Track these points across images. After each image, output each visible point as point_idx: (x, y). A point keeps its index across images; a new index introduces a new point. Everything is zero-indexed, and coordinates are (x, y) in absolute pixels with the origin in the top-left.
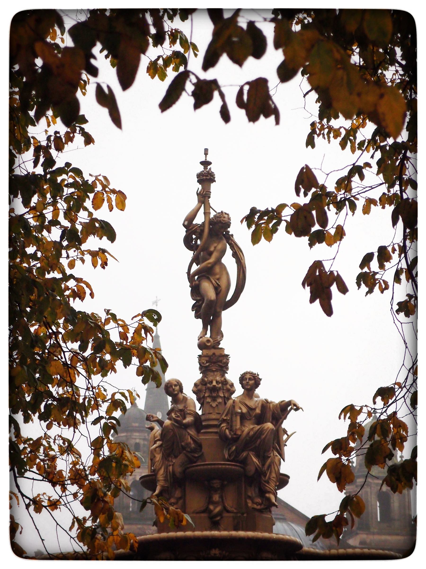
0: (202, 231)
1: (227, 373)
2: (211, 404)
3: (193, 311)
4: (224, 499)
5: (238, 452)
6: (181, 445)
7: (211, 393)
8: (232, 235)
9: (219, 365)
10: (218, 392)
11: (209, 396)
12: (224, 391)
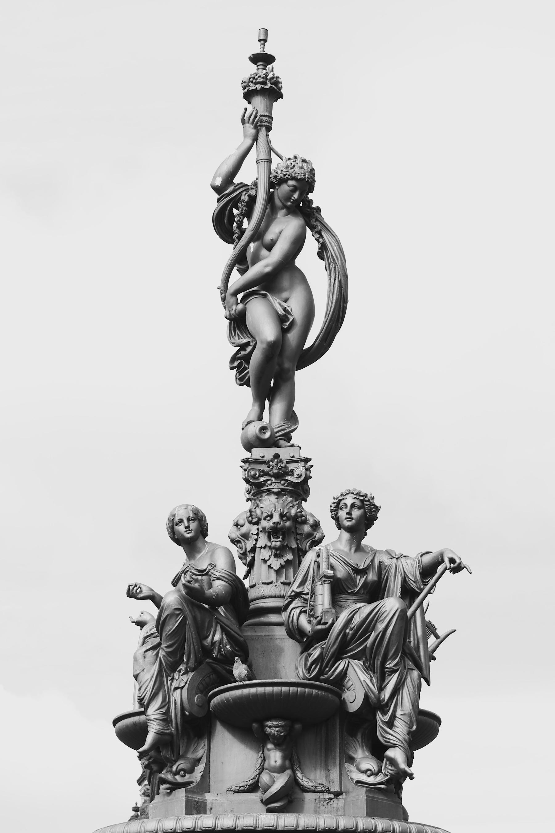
0: (253, 199)
1: (306, 501)
3: (232, 368)
7: (270, 539)
8: (318, 209)
9: (287, 480)
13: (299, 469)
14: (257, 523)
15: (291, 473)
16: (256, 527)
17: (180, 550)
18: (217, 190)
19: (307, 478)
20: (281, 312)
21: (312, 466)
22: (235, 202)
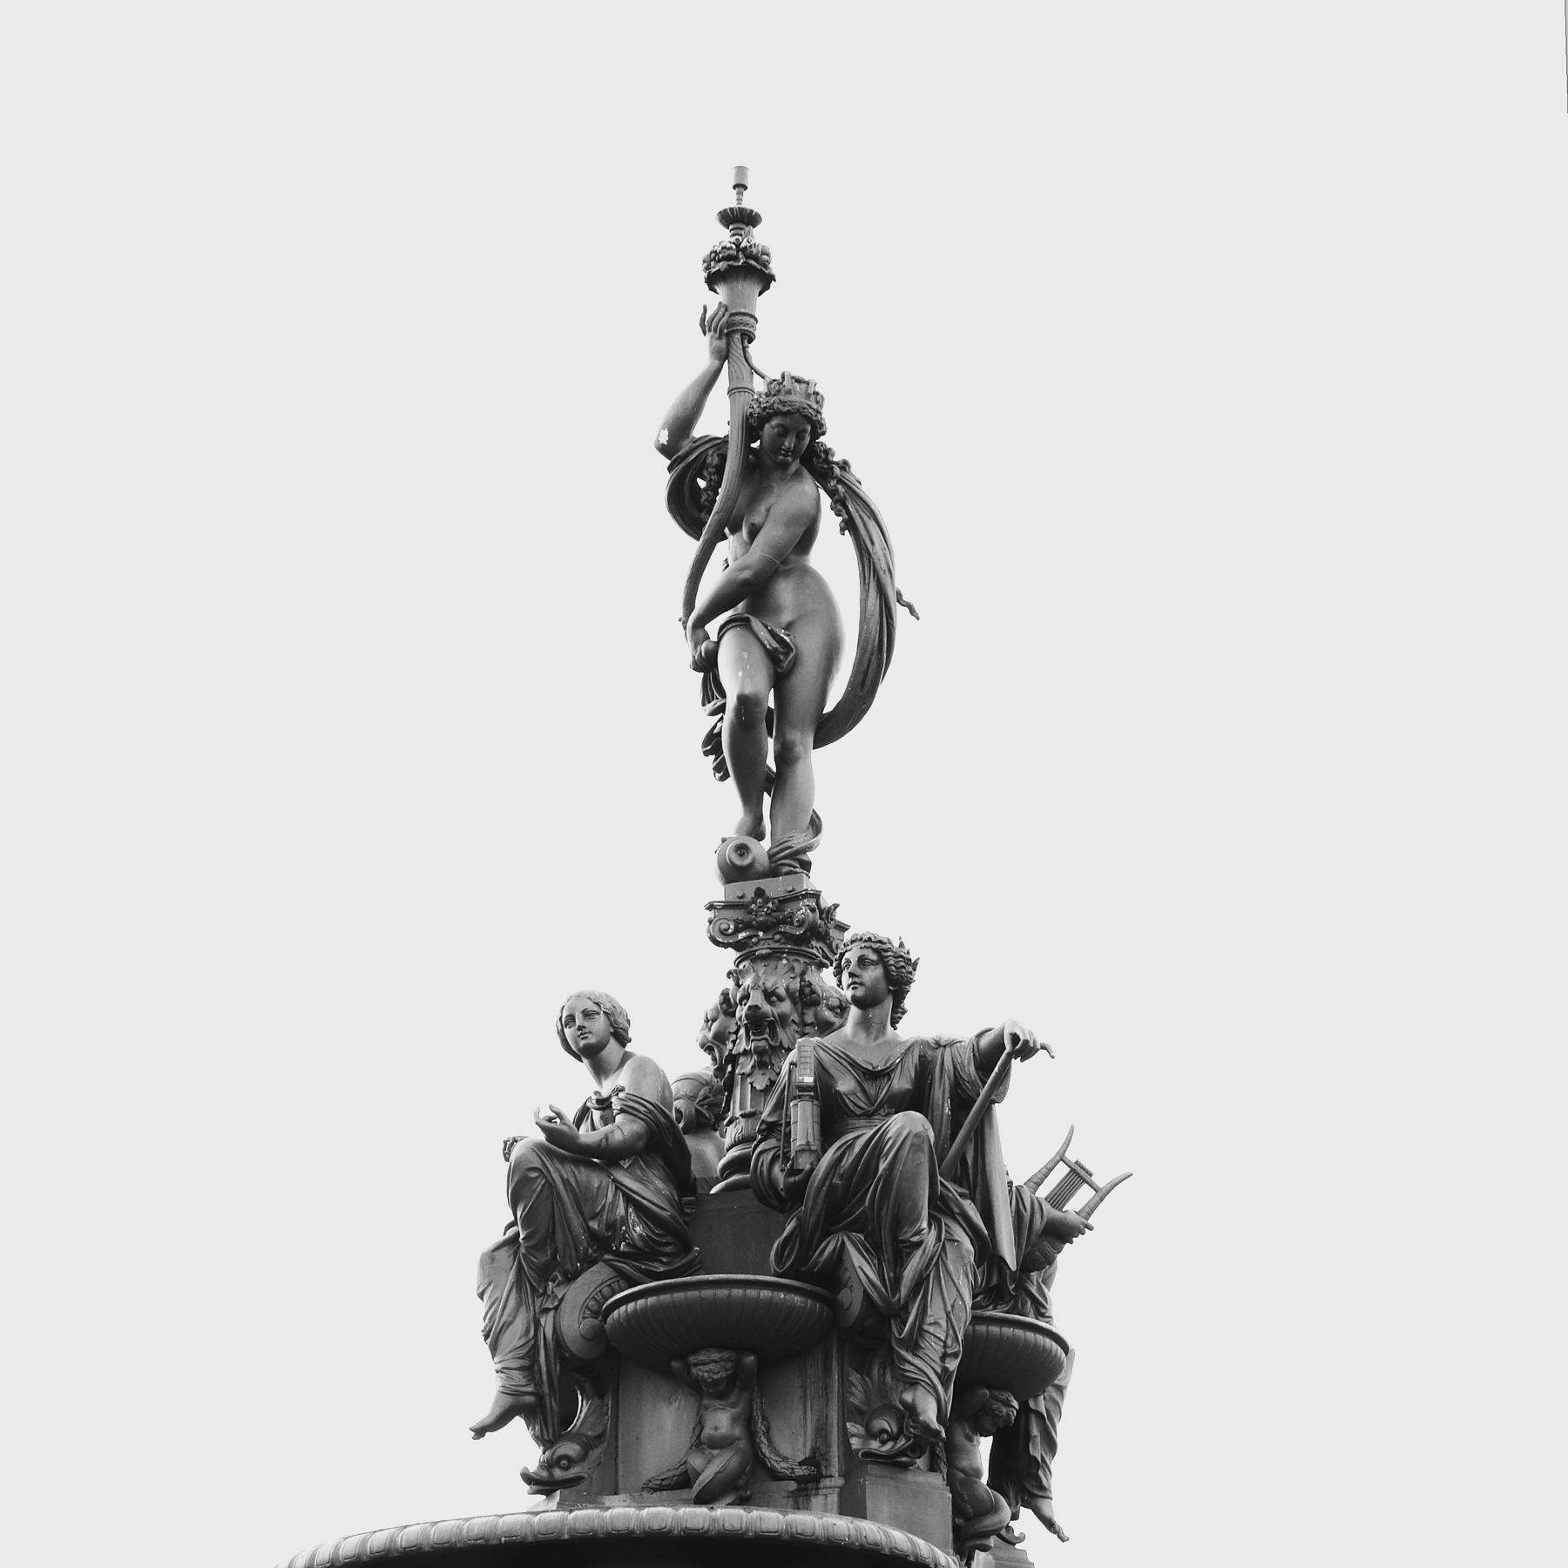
4: (761, 1427)
5: (806, 1240)
6: (589, 1230)
8: (844, 466)
10: (773, 1034)
17: (584, 1067)
18: (665, 450)
20: (771, 643)
22: (698, 467)
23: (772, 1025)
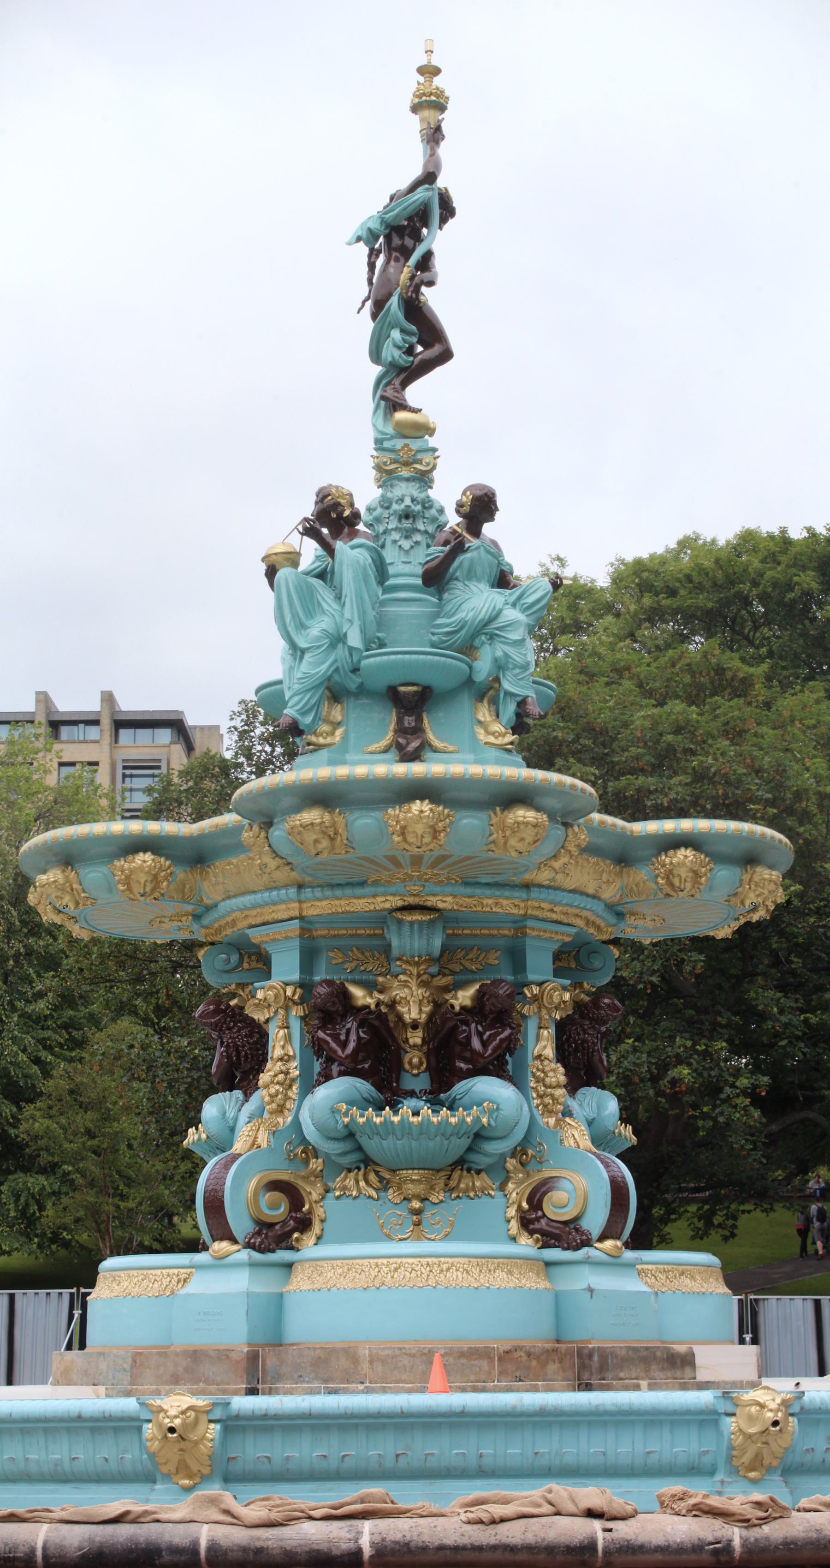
1: (431, 488)
2: (399, 543)
11: (396, 529)
12: (425, 520)
13: (427, 458)
14: (388, 508)
15: (420, 462)
16: (387, 511)
19: (434, 467)
21: (438, 457)
23: (414, 517)
